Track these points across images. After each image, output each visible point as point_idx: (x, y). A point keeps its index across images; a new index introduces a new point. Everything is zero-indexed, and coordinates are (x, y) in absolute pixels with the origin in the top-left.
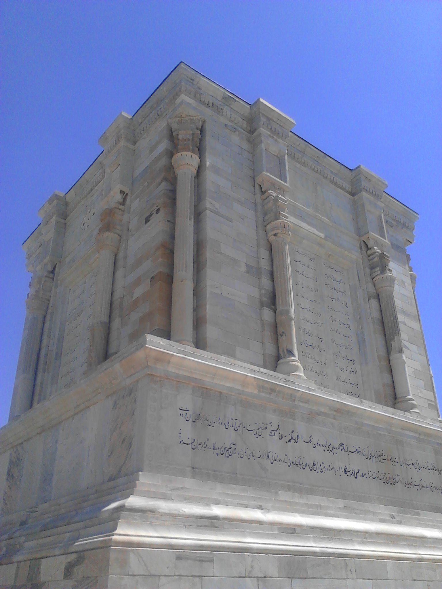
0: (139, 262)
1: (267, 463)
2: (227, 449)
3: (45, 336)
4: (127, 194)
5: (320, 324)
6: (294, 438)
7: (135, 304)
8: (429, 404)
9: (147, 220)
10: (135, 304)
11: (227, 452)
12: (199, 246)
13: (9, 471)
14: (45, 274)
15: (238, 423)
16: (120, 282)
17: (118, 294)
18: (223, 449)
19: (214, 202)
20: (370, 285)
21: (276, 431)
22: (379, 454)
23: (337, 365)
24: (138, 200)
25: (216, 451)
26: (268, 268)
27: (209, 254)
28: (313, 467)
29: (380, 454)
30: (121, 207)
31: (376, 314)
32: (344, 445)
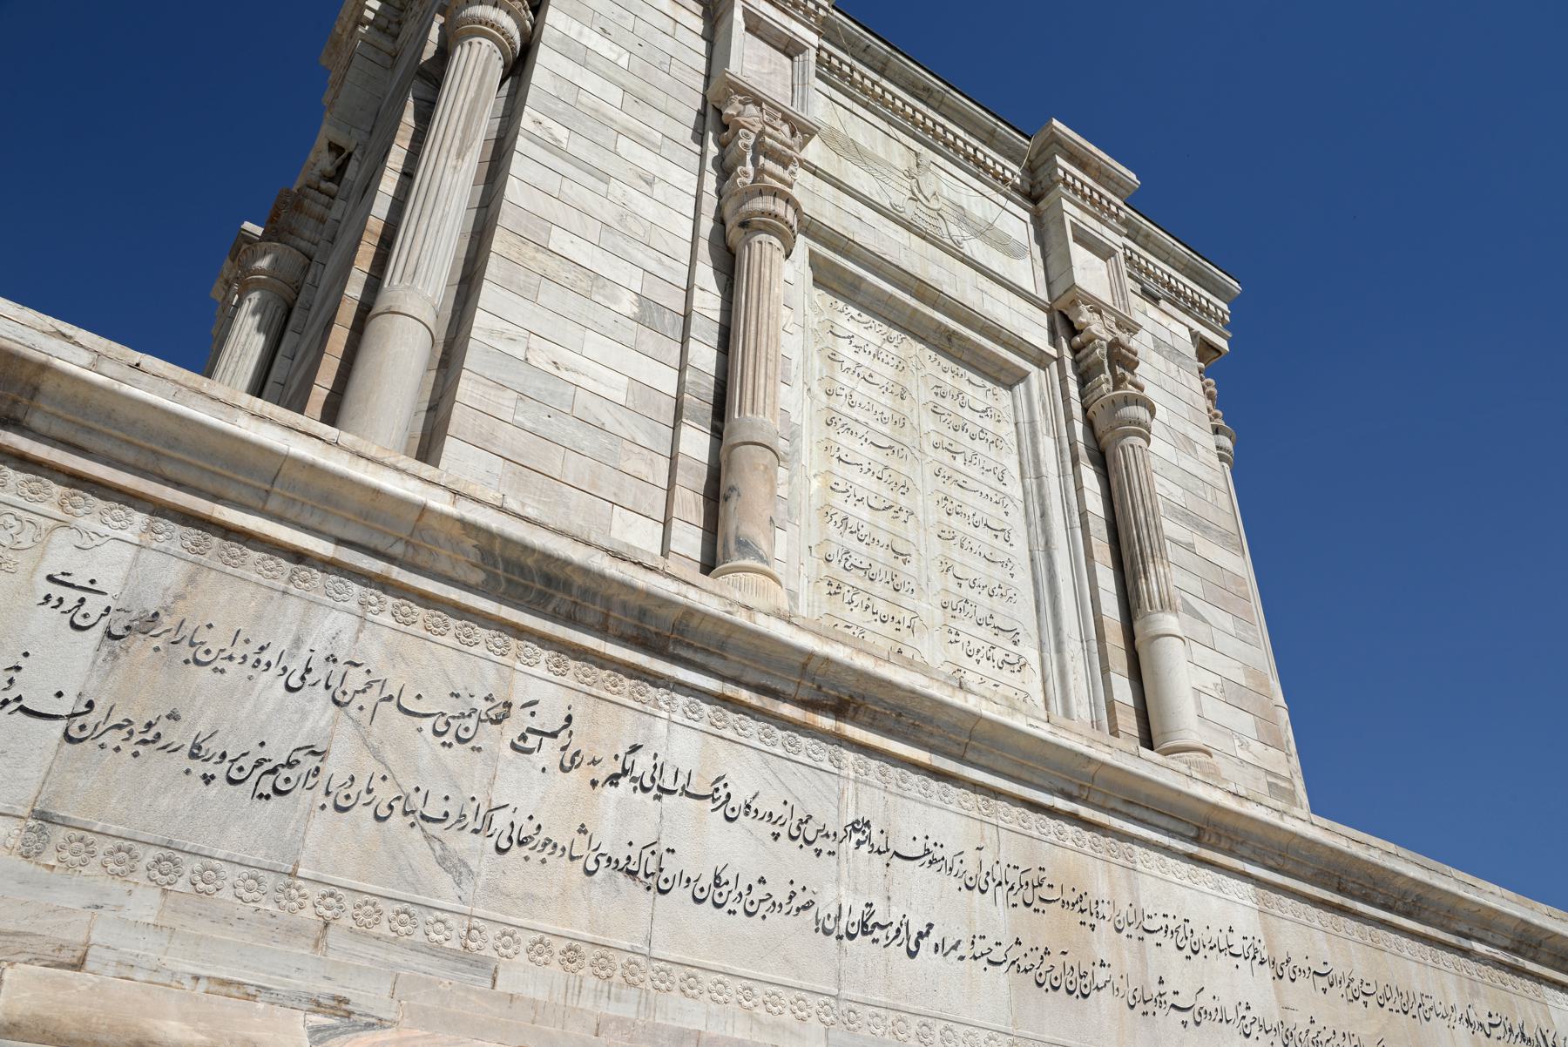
2: (267, 766)
4: (350, 155)
5: (903, 516)
6: (637, 773)
8: (1270, 784)
11: (272, 778)
15: (357, 679)
18: (247, 763)
19: (548, 122)
21: (554, 735)
22: (1026, 878)
23: (953, 637)
25: (199, 768)
28: (713, 892)
29: (1031, 877)
30: (332, 186)
32: (875, 830)
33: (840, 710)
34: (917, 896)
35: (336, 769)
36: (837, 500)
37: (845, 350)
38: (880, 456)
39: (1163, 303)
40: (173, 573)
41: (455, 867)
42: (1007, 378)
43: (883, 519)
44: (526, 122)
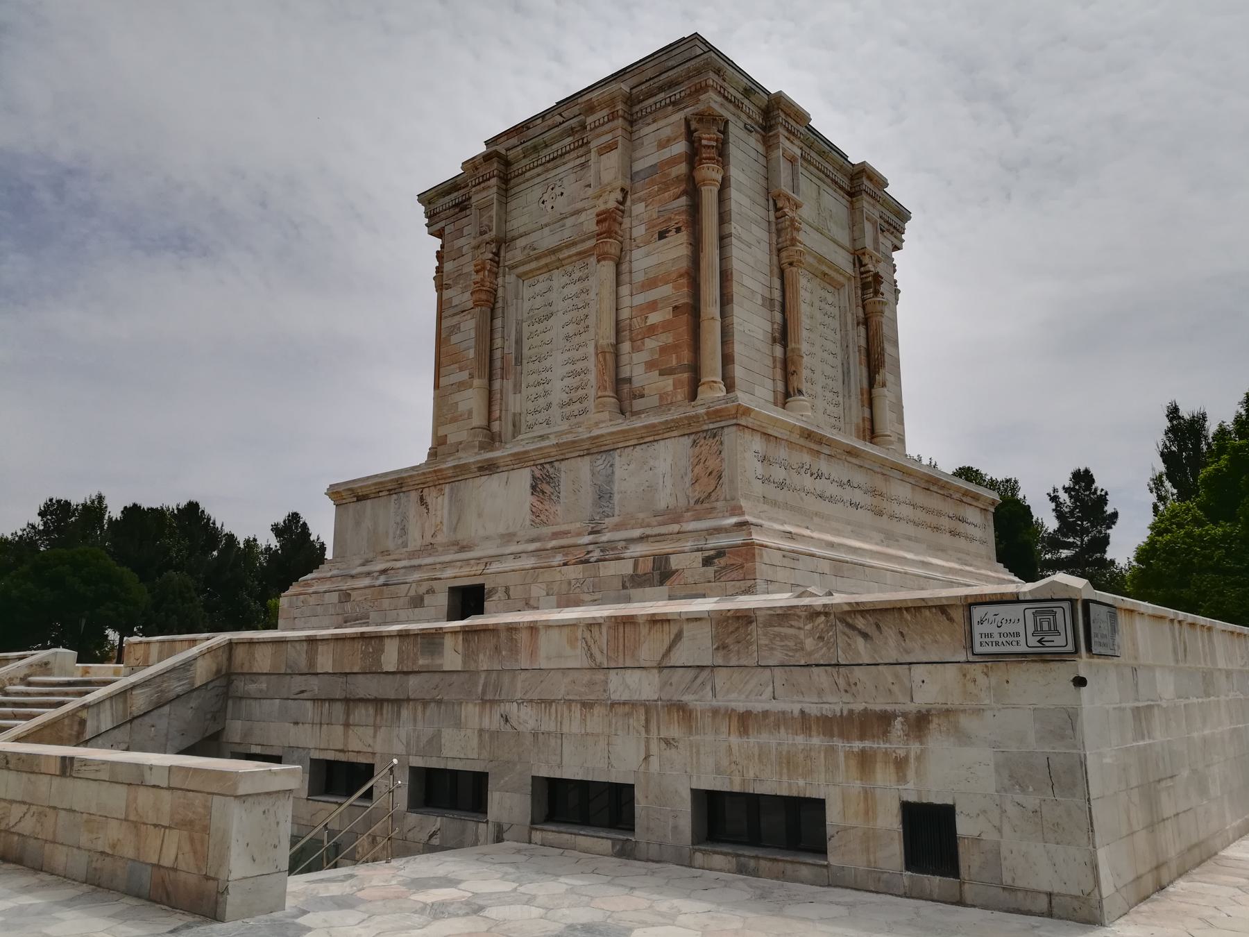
0: (651, 284)
3: (498, 335)
7: (652, 330)
9: (662, 235)
10: (652, 330)
11: (781, 485)
12: (725, 277)
13: (534, 488)
14: (491, 256)
16: (626, 301)
17: (625, 314)
20: (860, 309)
24: (643, 204)
26: (780, 299)
27: (736, 289)
28: (831, 499)
31: (863, 343)
34: (858, 496)
42: (837, 286)
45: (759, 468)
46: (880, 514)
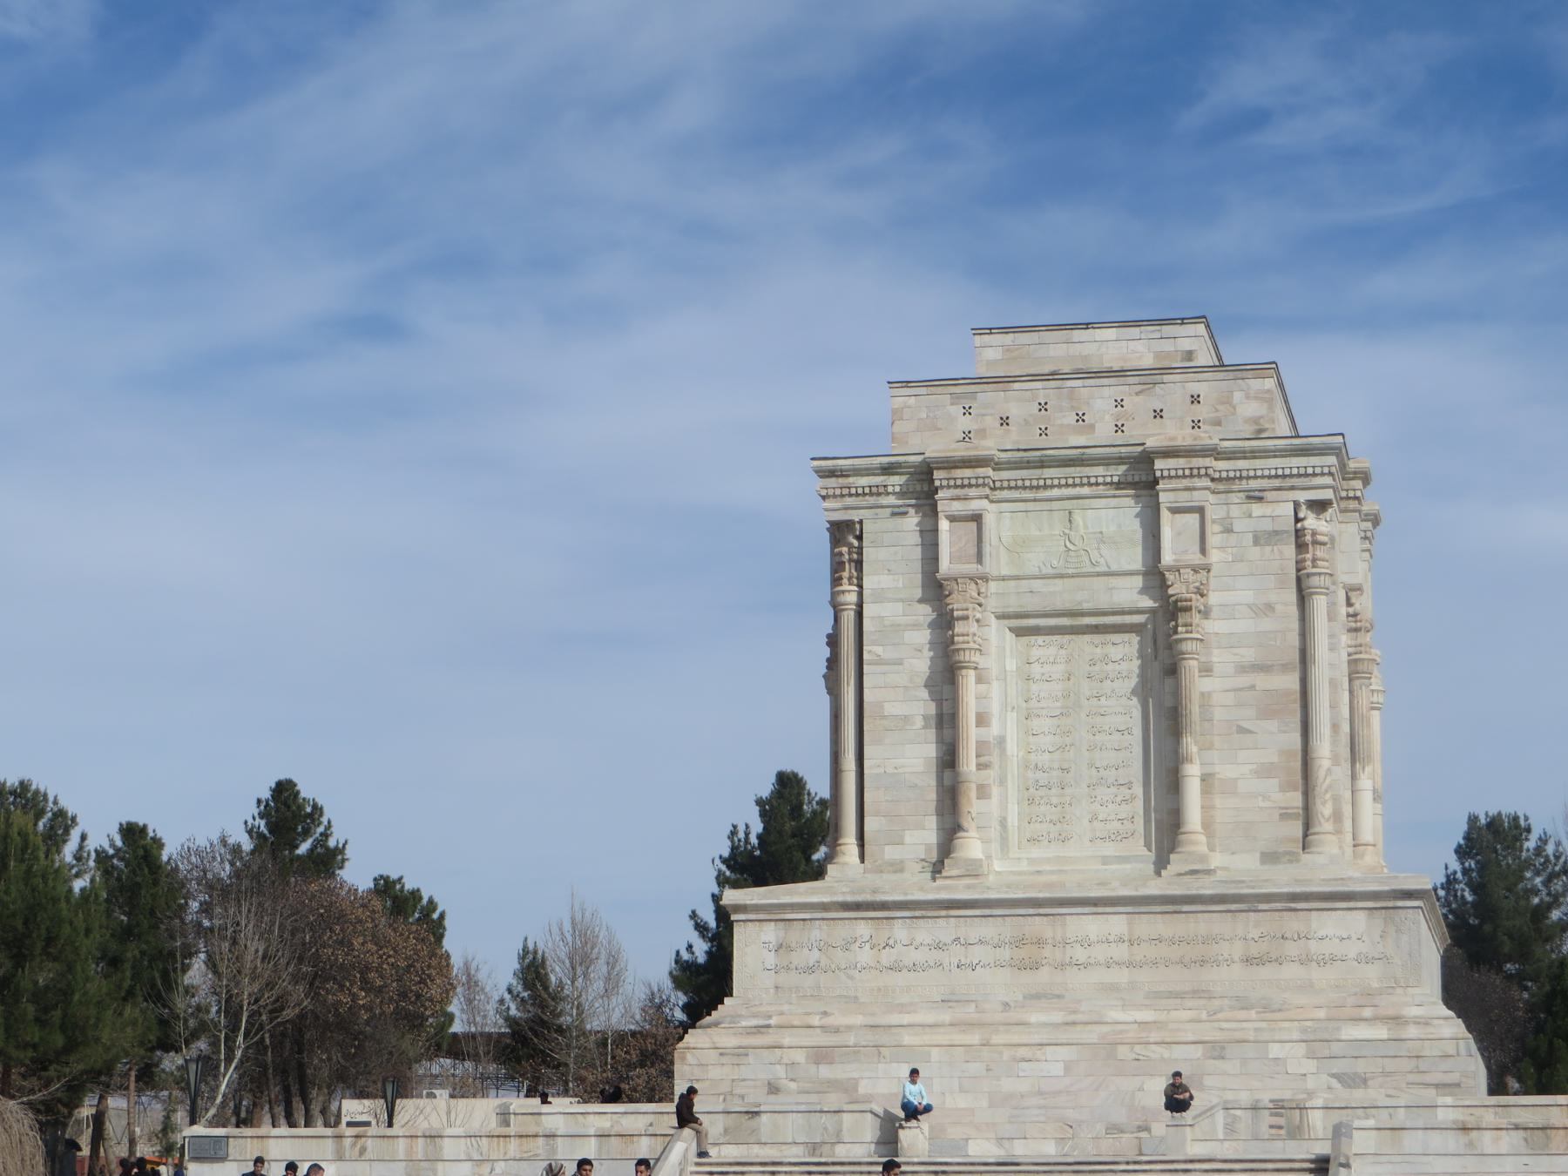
1: (855, 973)
11: (810, 970)
28: (914, 967)
33: (948, 908)
35: (823, 964)
36: (1032, 756)
37: (1036, 669)
38: (1055, 721)
39: (1269, 495)
40: (782, 934)
41: (851, 978)
43: (1056, 756)
44: (866, 656)
45: (771, 959)
46: (1035, 966)
